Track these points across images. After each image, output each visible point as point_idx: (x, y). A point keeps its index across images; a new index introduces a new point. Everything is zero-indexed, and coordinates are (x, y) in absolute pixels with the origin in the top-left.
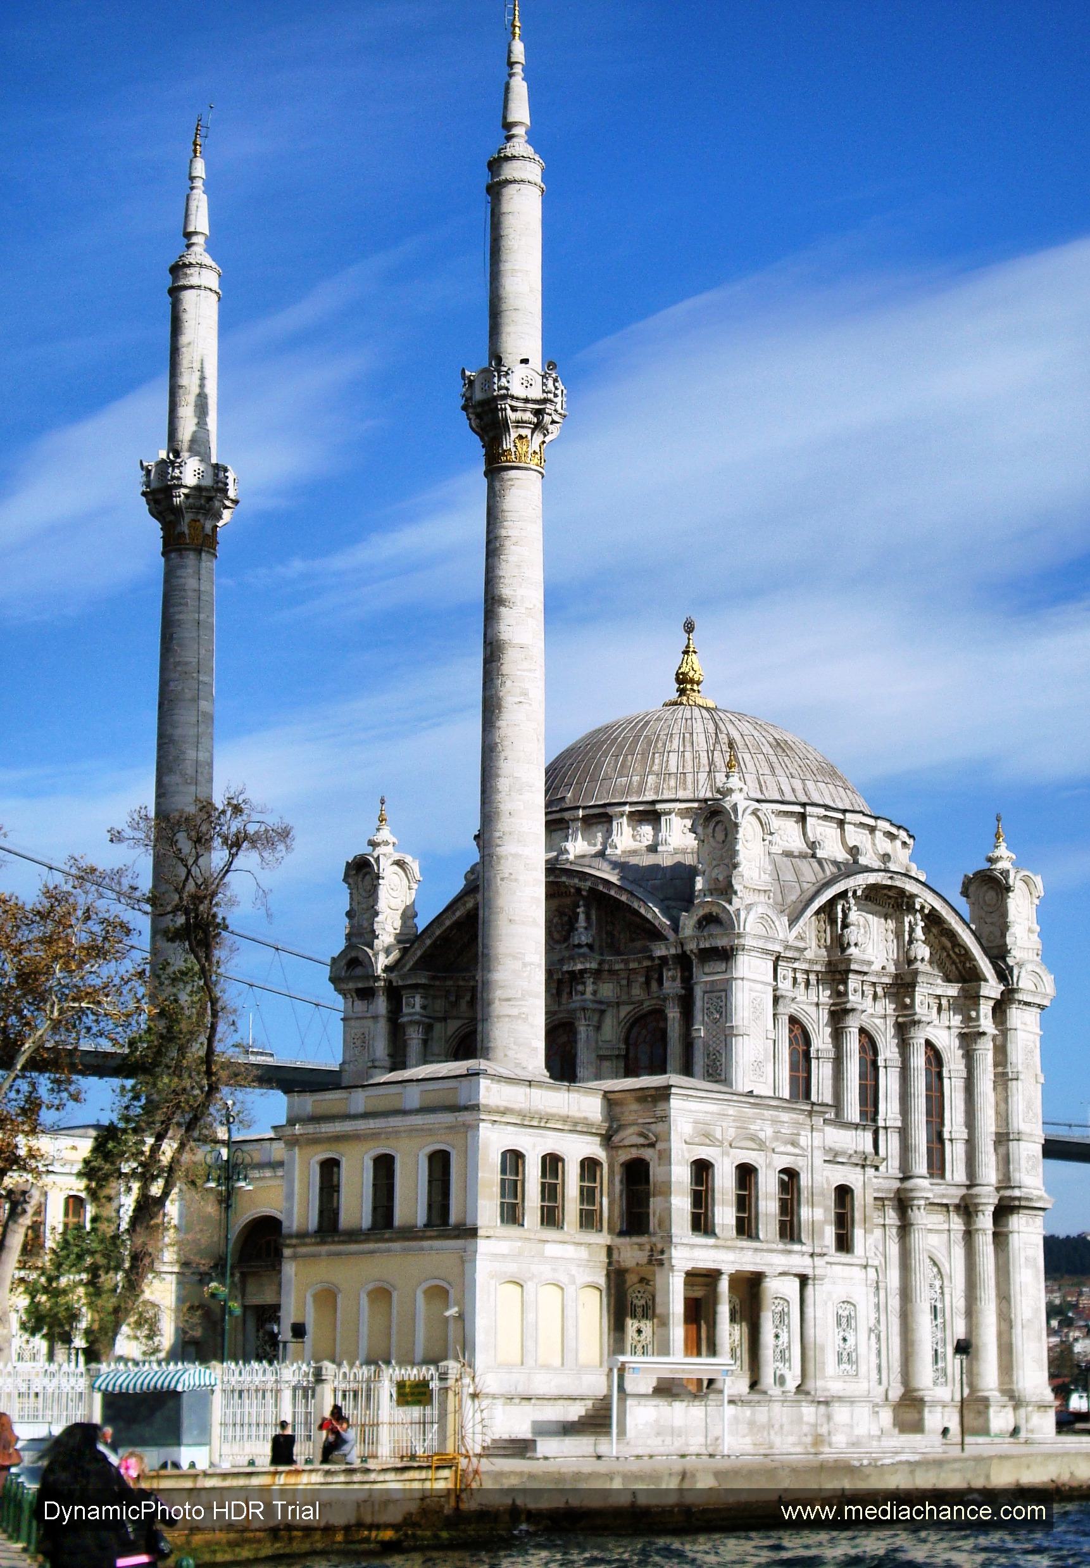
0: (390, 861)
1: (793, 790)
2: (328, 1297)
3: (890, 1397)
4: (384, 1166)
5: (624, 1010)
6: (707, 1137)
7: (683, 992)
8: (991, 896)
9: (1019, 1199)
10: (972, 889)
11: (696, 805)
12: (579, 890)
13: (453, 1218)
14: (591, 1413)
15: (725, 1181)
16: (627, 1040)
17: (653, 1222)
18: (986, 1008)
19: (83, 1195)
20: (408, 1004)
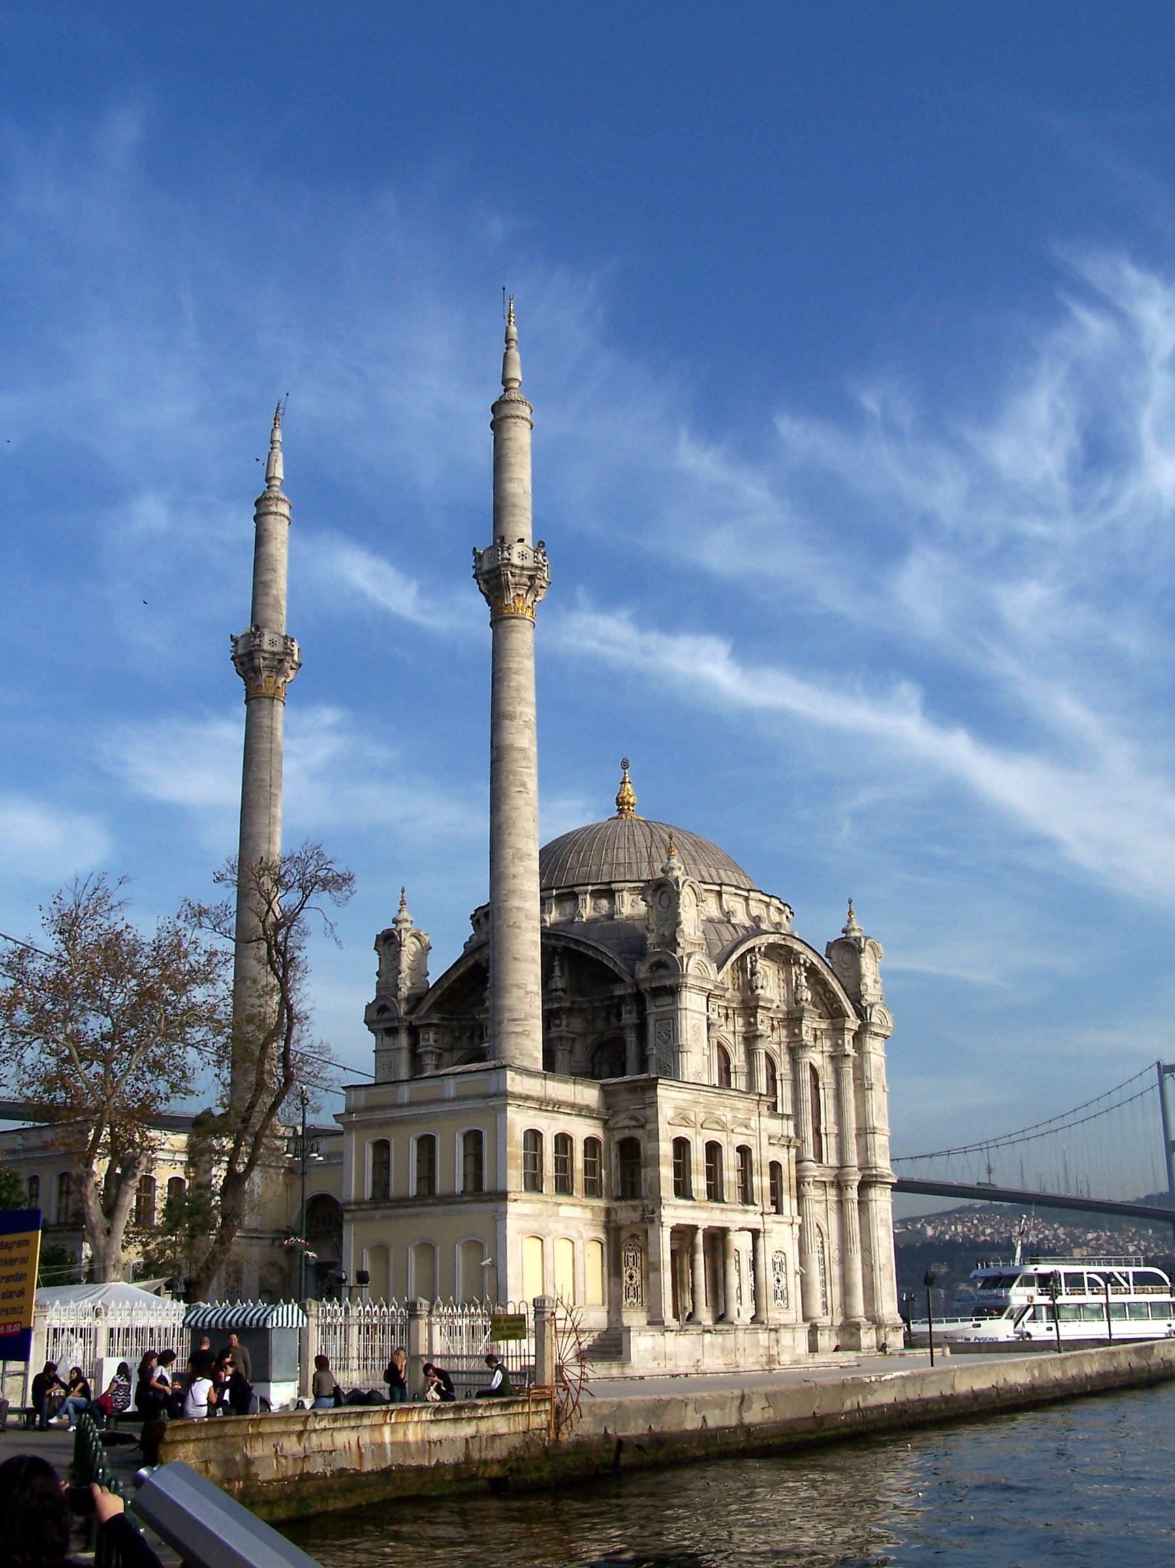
0: (409, 934)
1: (710, 875)
2: (381, 1251)
3: (835, 1324)
4: (427, 1144)
5: (590, 1039)
6: (685, 1121)
7: (638, 1021)
8: (847, 956)
9: (876, 1176)
10: (833, 953)
11: (641, 885)
12: (555, 948)
13: (486, 1187)
14: (598, 1342)
15: (698, 1156)
16: (592, 1061)
17: (644, 1190)
18: (848, 1037)
19: (183, 1177)
20: (424, 1039)
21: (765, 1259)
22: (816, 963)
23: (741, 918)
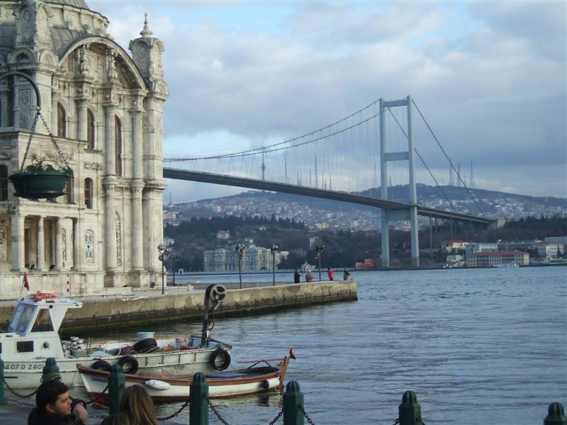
7: (8, 90)
8: (142, 50)
9: (154, 185)
10: (134, 47)
18: (140, 100)
21: (81, 234)
22: (121, 54)
23: (75, 26)
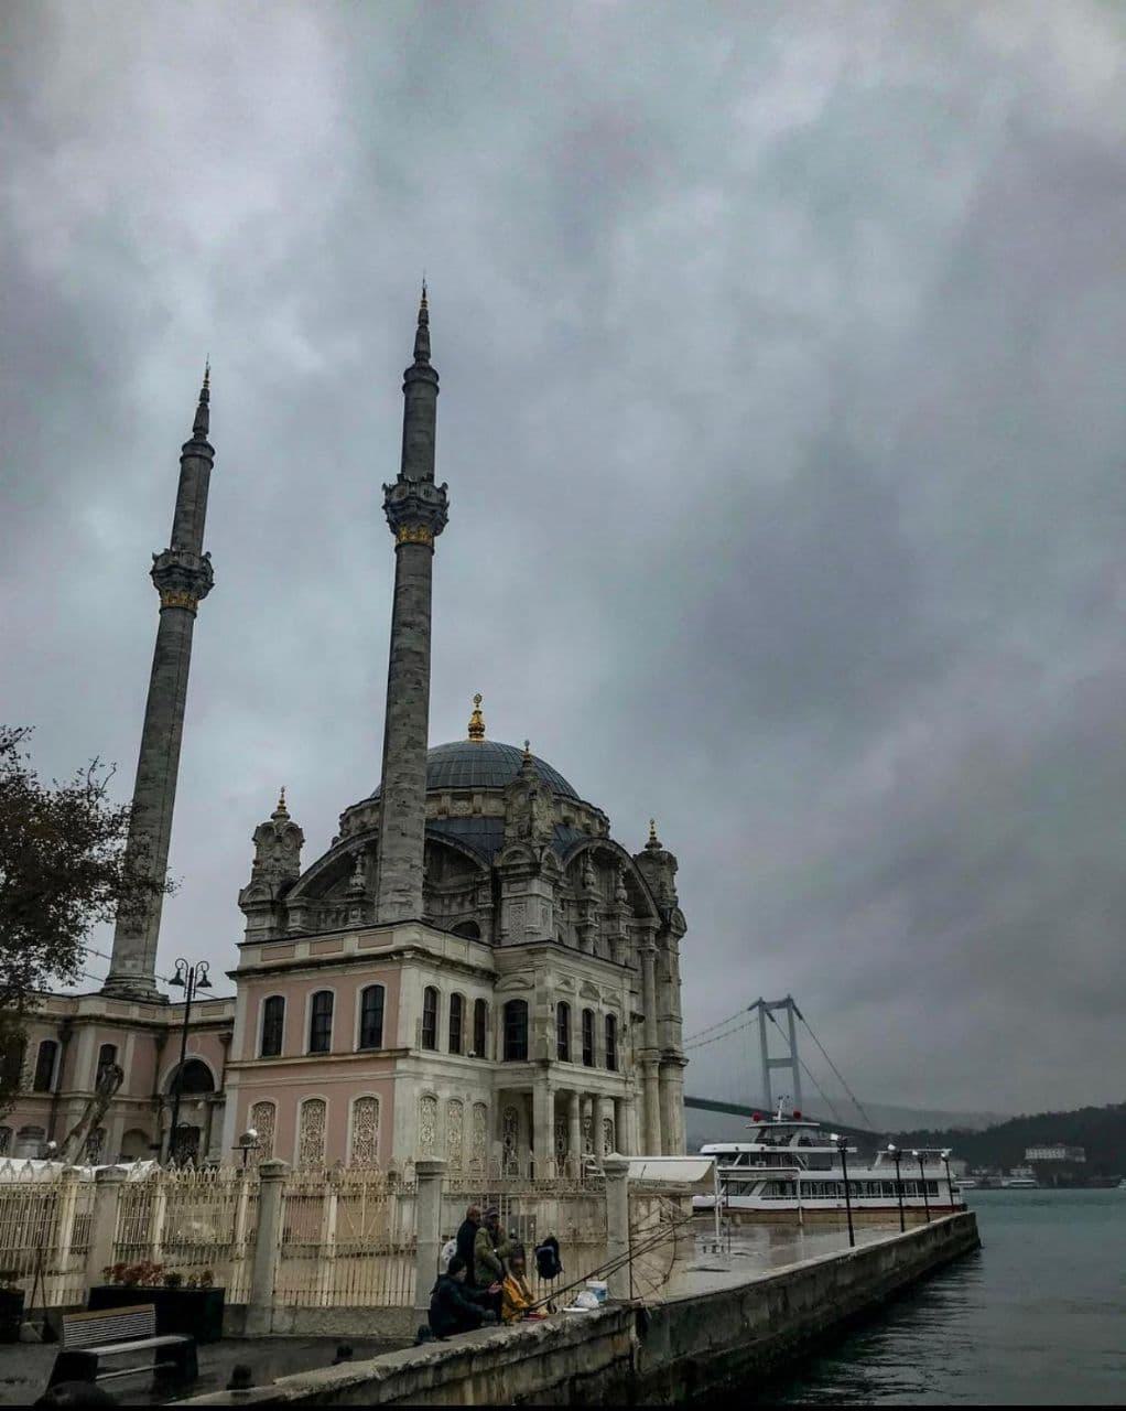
7: (493, 906)
15: (576, 1020)
19: (55, 1039)
